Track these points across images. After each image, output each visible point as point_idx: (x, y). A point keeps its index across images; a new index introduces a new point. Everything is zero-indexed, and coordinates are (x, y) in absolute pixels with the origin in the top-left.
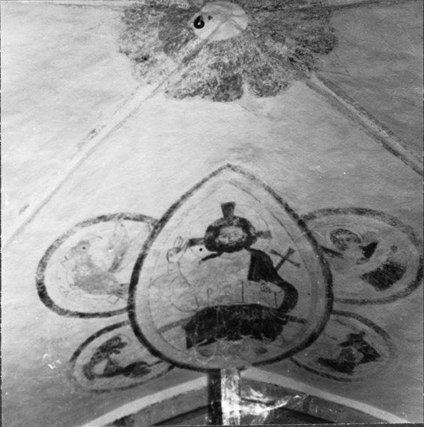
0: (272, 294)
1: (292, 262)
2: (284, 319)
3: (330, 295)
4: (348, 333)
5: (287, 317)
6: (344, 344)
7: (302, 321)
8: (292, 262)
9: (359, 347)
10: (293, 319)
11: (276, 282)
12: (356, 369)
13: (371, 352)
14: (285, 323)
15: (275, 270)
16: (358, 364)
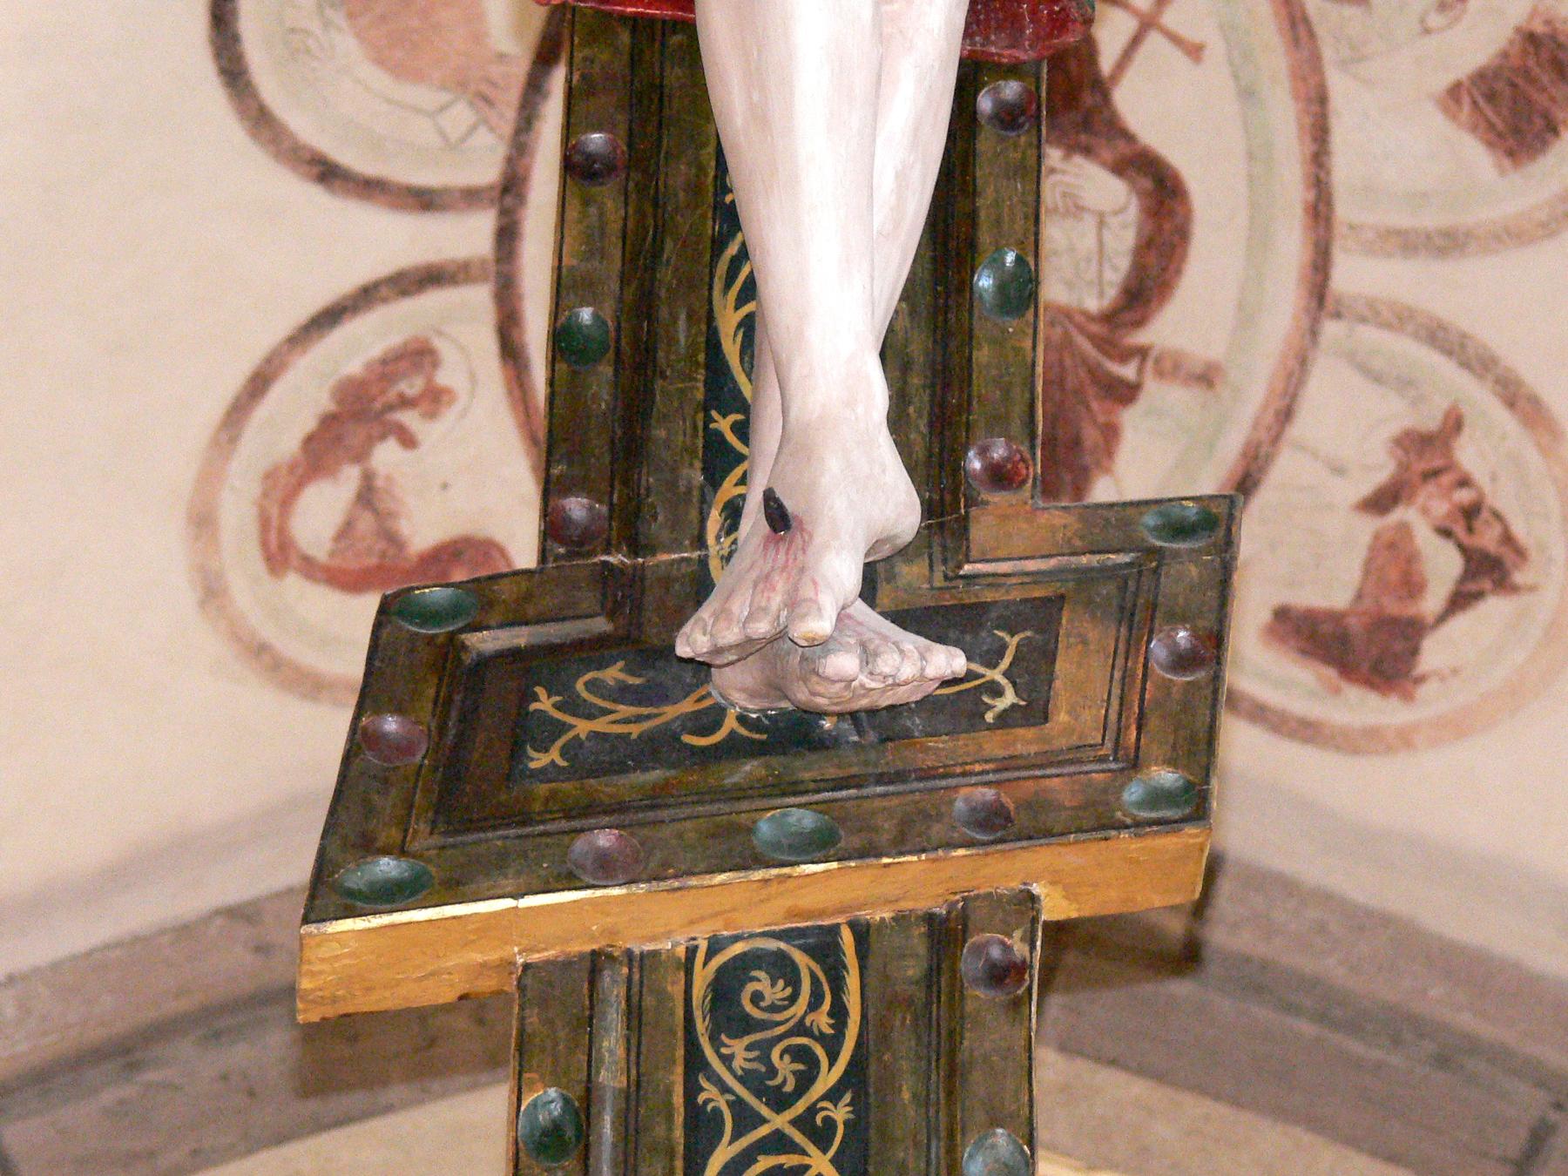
0: (1089, 222)
1: (1175, 39)
2: (1128, 371)
3: (1320, 211)
4: (1394, 428)
5: (1142, 353)
6: (1381, 501)
7: (1207, 377)
8: (1175, 39)
9: (1440, 508)
10: (1173, 368)
11: (1107, 155)
12: (1433, 653)
13: (1487, 538)
14: (1126, 393)
15: (1102, 88)
16: (1442, 618)
